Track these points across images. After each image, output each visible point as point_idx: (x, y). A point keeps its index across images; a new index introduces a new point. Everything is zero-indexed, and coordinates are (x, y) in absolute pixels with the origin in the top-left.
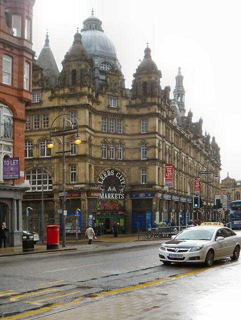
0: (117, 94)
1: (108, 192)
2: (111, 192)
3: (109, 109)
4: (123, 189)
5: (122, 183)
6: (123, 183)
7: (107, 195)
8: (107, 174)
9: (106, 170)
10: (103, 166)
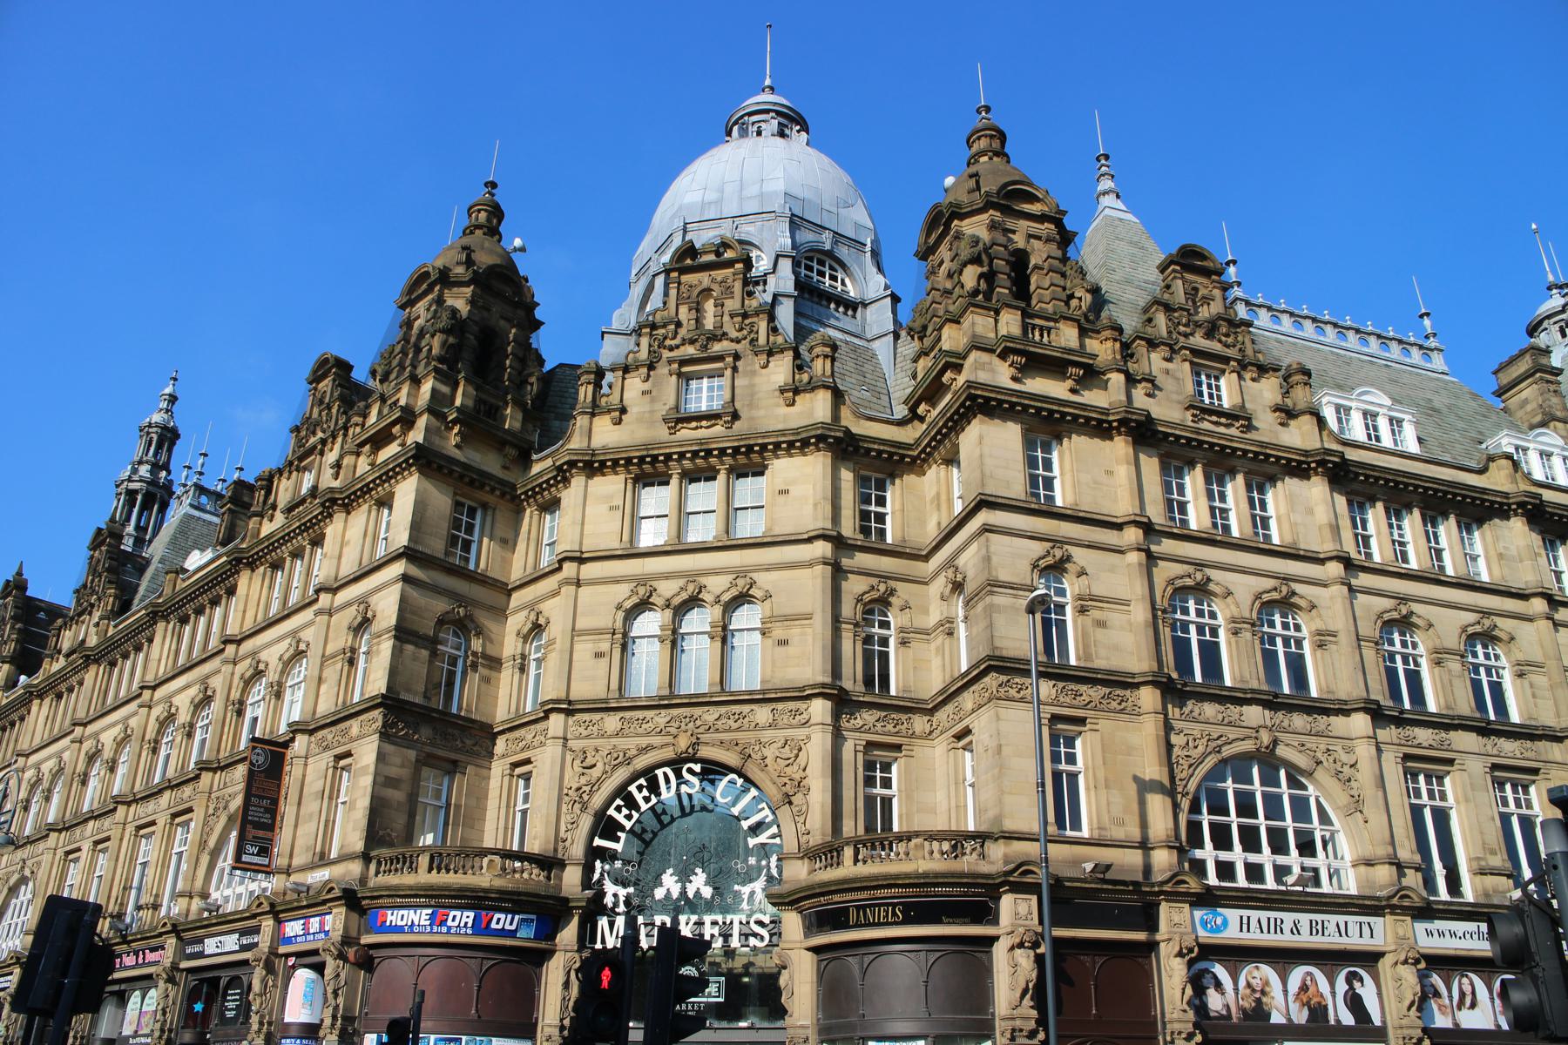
3: (673, 430)
6: (763, 838)
9: (641, 763)
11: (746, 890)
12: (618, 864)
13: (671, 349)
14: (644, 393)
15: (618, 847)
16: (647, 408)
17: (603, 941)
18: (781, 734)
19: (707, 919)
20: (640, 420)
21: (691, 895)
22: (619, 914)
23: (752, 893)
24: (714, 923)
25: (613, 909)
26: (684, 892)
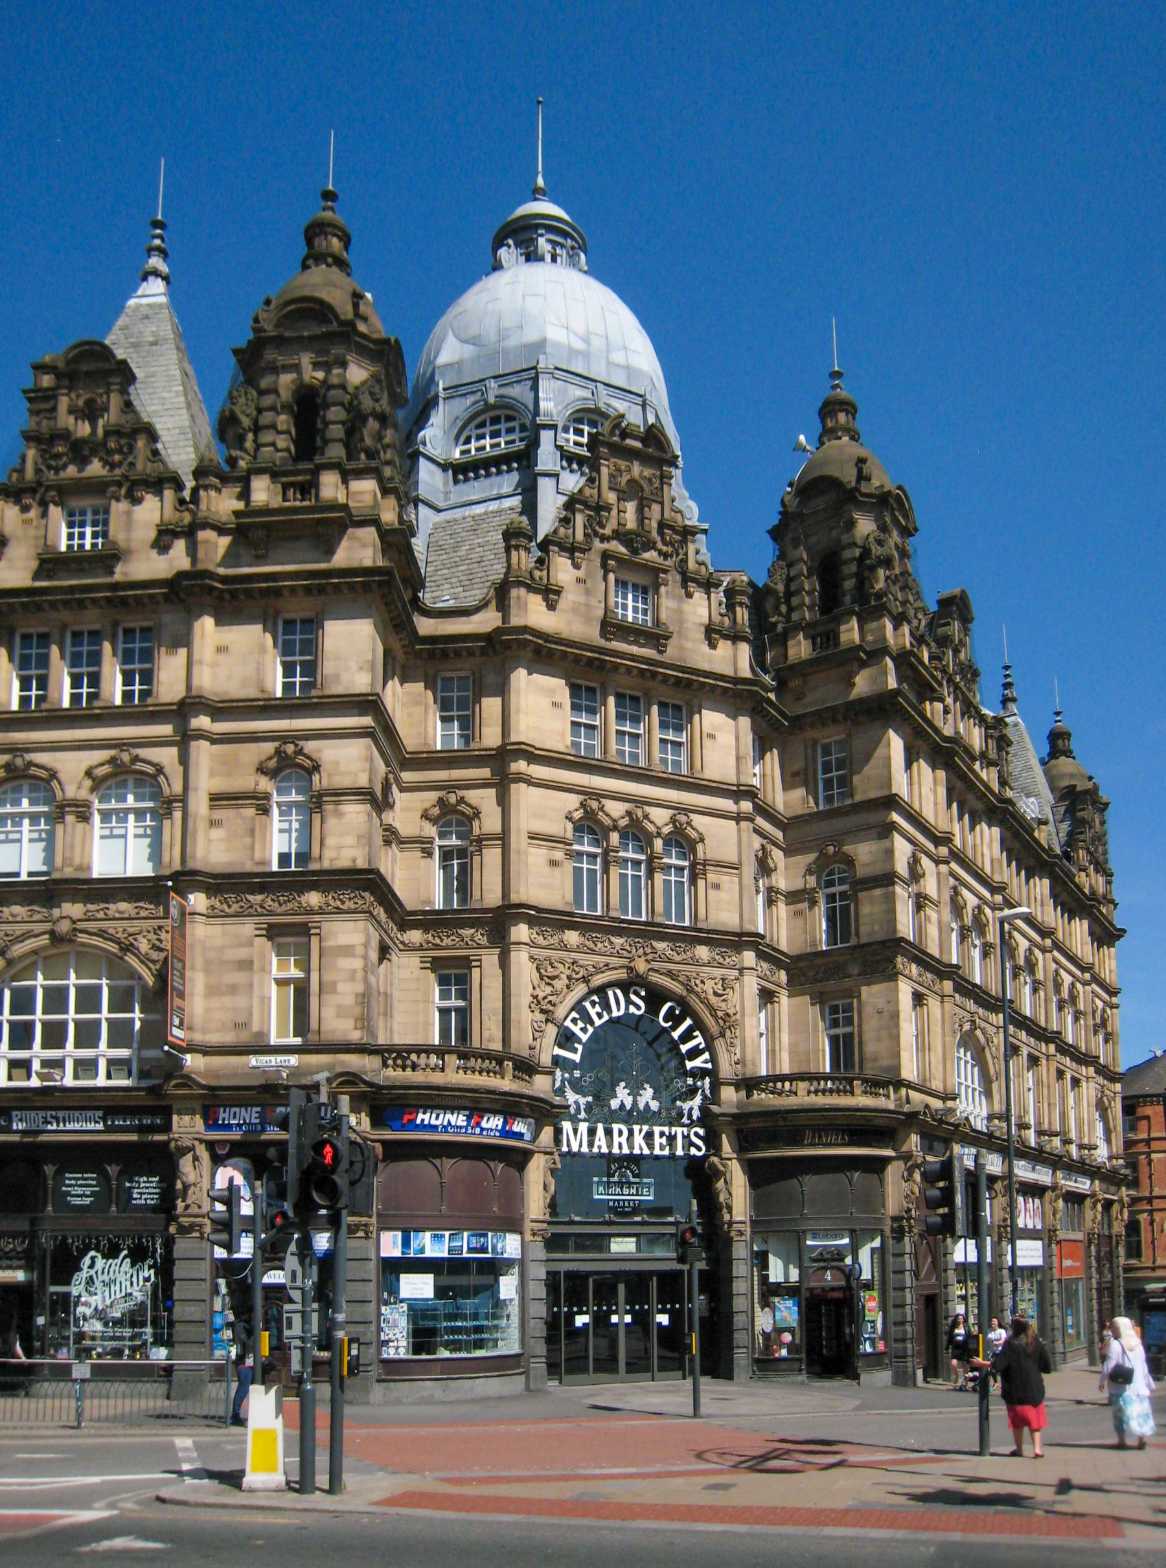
0: (650, 555)
1: (611, 1117)
2: (630, 1116)
4: (698, 1100)
5: (689, 1065)
6: (698, 1062)
7: (608, 1132)
8: (606, 1007)
9: (598, 980)
10: (587, 960)
11: (686, 1106)
12: (577, 1074)
13: (604, 538)
14: (578, 580)
15: (576, 1058)
16: (582, 599)
17: (569, 1145)
18: (718, 972)
19: (657, 1130)
20: (575, 610)
21: (641, 1106)
22: (580, 1120)
23: (691, 1109)
24: (662, 1134)
25: (575, 1115)
26: (635, 1103)
